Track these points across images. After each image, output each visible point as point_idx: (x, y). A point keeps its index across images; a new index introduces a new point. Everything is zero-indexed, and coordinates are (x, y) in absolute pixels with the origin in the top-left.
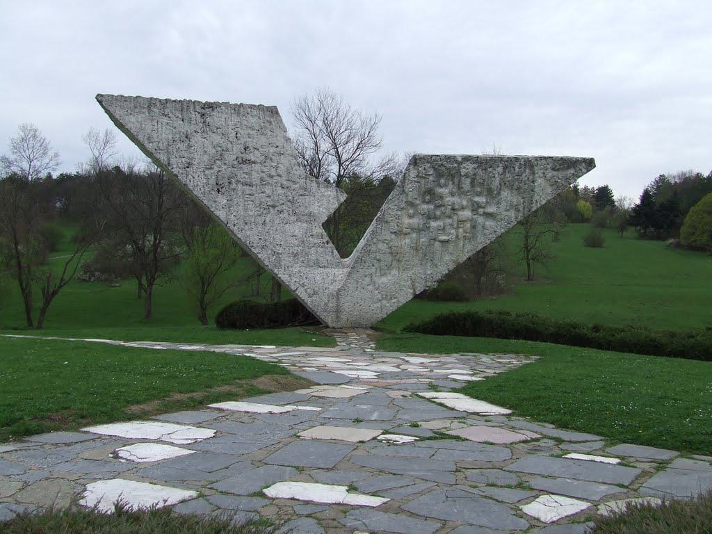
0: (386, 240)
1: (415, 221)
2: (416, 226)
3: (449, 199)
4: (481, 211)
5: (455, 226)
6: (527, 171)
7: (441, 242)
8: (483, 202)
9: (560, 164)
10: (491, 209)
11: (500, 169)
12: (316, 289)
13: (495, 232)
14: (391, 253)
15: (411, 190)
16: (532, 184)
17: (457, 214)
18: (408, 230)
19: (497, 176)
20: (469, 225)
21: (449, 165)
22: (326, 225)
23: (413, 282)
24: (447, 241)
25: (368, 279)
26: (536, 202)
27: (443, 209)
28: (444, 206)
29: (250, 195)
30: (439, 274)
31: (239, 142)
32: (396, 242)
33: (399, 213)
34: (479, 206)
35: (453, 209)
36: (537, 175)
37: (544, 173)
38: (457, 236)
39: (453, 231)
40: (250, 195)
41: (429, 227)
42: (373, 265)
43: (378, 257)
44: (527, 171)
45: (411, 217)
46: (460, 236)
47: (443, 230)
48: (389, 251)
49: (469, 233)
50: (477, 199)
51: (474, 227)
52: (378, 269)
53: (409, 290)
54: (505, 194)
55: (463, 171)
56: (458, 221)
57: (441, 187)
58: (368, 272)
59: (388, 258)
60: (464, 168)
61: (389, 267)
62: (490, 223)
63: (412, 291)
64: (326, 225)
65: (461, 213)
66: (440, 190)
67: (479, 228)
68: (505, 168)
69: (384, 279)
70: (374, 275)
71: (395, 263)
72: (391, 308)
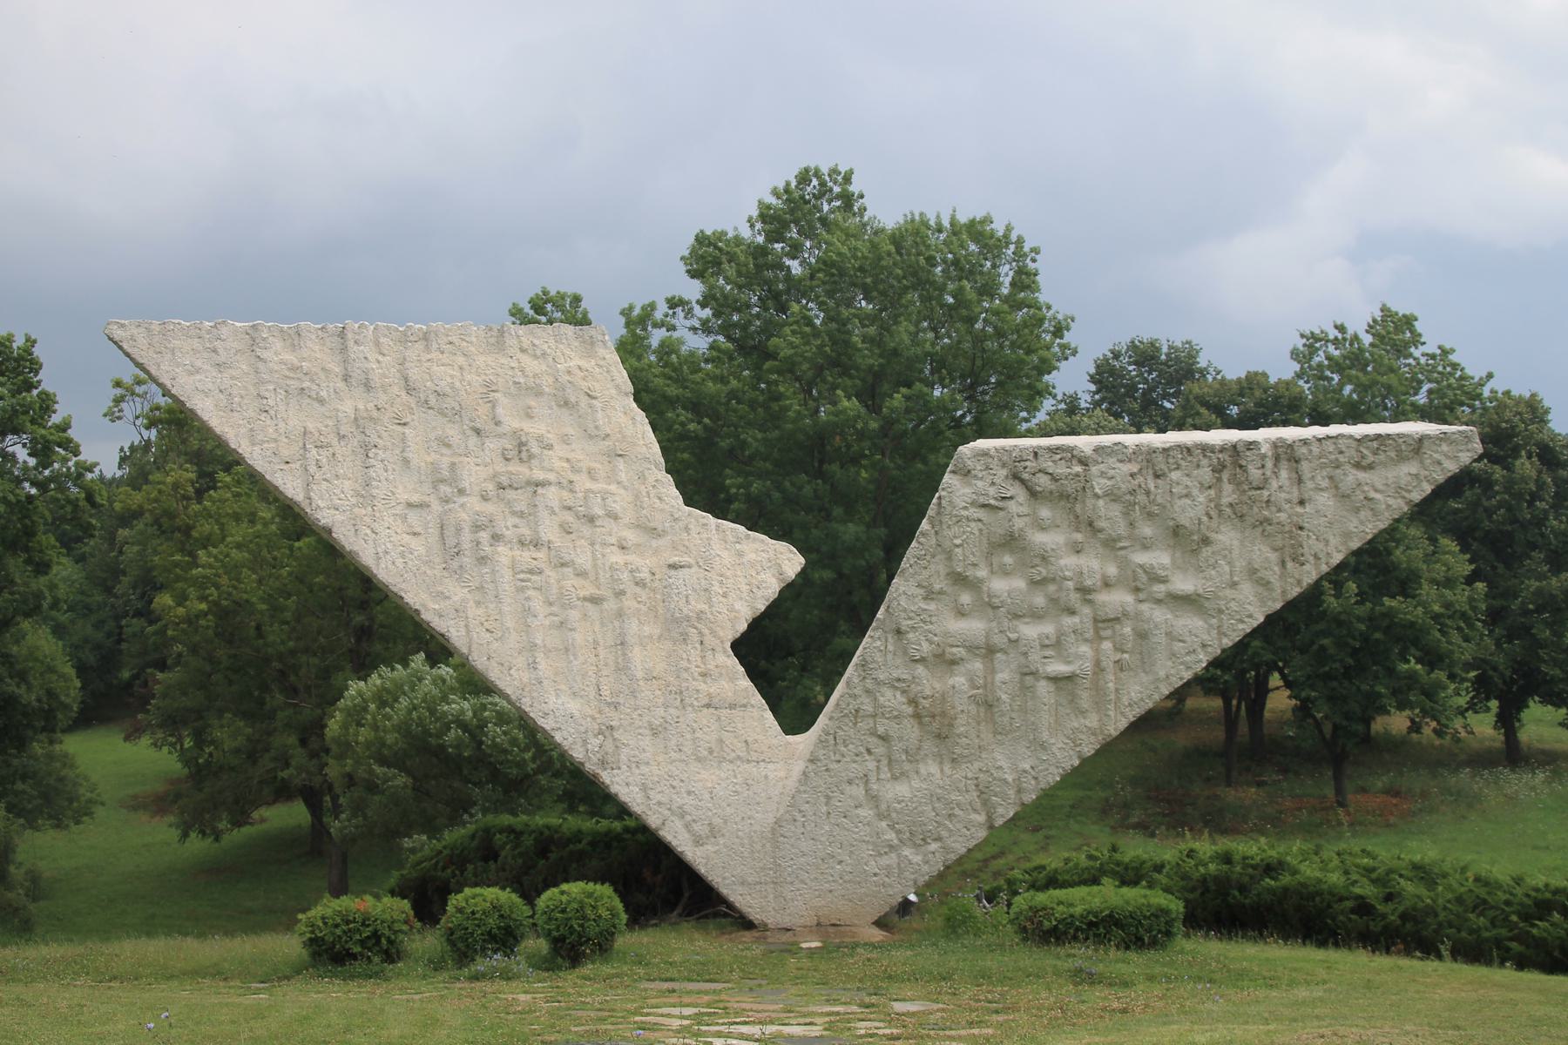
0: (899, 680)
1: (974, 627)
2: (982, 641)
3: (1069, 562)
4: (1159, 589)
5: (1090, 634)
6: (1284, 474)
7: (1055, 679)
8: (1164, 568)
10: (1184, 584)
12: (717, 821)
13: (1204, 646)
14: (917, 716)
15: (958, 542)
16: (1299, 509)
17: (1090, 602)
18: (960, 652)
20: (1128, 630)
21: (1061, 470)
22: (744, 648)
23: (983, 792)
24: (1070, 678)
25: (858, 791)
26: (1316, 556)
27: (1052, 588)
28: (1054, 580)
29: (531, 572)
30: (1053, 769)
31: (500, 430)
32: (928, 682)
33: (932, 606)
34: (1157, 579)
35: (1084, 591)
36: (1310, 484)
37: (1331, 478)
38: (1098, 663)
39: (1085, 649)
40: (531, 572)
41: (1017, 641)
42: (869, 751)
43: (881, 730)
44: (1284, 474)
45: (961, 613)
46: (1108, 663)
47: (1057, 645)
48: (910, 710)
49: (1131, 652)
50: (1141, 558)
51: (1142, 636)
52: (885, 762)
53: (974, 816)
54: (1227, 537)
55: (1099, 485)
56: (1096, 621)
57: (1043, 529)
58: (855, 769)
59: (910, 731)
60: (1103, 474)
61: (913, 756)
62: (1190, 624)
63: (981, 818)
64: (744, 648)
65: (1102, 597)
66: (1040, 538)
67: (1159, 638)
68: (1218, 469)
69: (902, 789)
70: (873, 779)
71: (929, 746)
72: (926, 868)
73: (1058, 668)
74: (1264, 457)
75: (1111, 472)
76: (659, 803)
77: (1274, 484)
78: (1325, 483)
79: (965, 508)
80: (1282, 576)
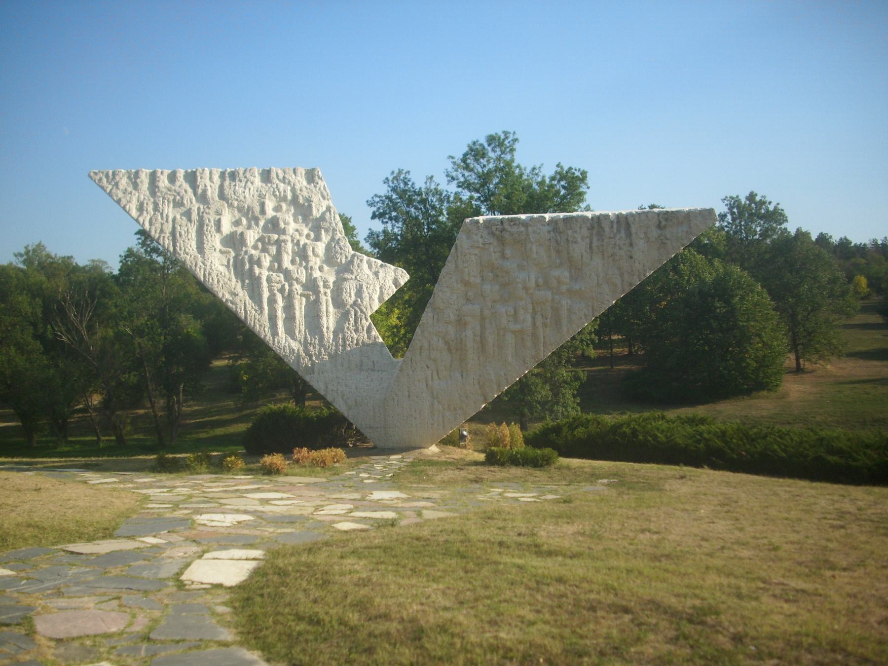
5: (530, 311)
7: (514, 332)
9: (666, 220)
11: (585, 232)
14: (450, 350)
19: (579, 240)
37: (645, 233)
38: (534, 324)
67: (564, 313)
73: (518, 327)
74: (612, 222)
75: (538, 231)
76: (332, 390)
77: (618, 236)
78: (642, 236)
79: (468, 249)
80: (623, 280)
